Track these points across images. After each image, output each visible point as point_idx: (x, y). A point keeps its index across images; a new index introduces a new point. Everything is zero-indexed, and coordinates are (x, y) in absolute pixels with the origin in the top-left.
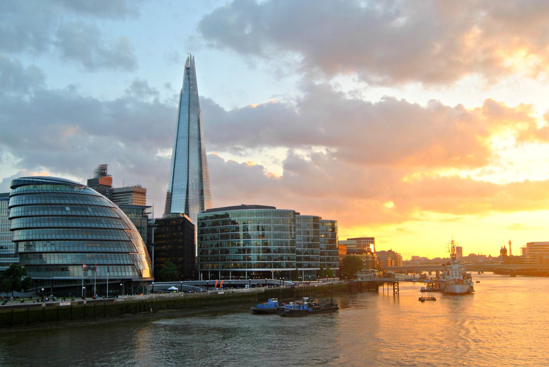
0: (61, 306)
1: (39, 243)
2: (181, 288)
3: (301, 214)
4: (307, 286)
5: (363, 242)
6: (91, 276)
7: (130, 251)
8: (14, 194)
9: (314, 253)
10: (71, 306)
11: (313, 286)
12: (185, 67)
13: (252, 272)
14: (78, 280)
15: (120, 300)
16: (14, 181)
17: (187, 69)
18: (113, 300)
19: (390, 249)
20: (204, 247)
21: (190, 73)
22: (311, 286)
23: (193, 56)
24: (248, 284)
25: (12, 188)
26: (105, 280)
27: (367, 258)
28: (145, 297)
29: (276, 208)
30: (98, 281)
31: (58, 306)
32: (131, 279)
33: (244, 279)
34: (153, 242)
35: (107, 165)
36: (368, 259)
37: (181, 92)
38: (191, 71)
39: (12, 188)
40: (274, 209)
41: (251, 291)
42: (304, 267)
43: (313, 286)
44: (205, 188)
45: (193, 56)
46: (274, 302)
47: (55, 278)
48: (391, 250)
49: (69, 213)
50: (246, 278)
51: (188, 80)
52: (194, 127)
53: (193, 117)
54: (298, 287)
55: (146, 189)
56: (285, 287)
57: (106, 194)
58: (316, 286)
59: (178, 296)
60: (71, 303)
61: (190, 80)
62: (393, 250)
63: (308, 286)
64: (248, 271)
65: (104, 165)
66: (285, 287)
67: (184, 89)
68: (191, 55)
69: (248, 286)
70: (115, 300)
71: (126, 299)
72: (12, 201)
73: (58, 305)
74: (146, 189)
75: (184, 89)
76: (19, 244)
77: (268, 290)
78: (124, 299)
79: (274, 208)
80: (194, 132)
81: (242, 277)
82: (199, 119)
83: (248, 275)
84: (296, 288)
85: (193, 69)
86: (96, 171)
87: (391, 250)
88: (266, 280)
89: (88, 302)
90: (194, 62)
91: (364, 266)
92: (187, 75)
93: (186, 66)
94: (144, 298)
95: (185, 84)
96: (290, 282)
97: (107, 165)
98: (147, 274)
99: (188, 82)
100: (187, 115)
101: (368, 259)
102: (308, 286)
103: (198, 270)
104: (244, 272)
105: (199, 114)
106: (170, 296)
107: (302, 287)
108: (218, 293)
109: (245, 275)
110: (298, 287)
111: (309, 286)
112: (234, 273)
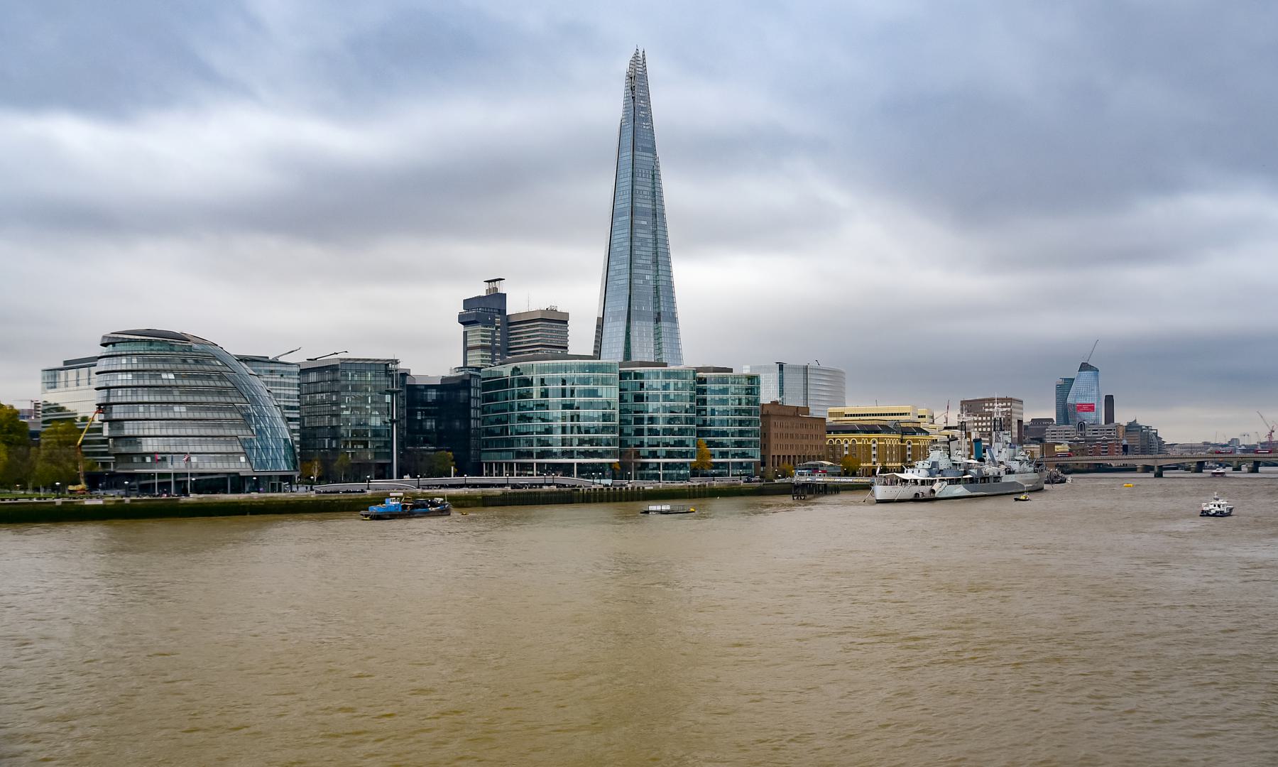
6: (183, 469)
7: (240, 434)
10: (115, 505)
11: (638, 488)
13: (544, 464)
18: (178, 499)
25: (103, 345)
26: (186, 475)
30: (176, 475)
31: (82, 506)
32: (237, 474)
33: (532, 475)
36: (880, 443)
43: (638, 488)
46: (394, 503)
50: (535, 474)
60: (104, 501)
62: (1140, 422)
71: (202, 498)
72: (102, 365)
73: (82, 504)
77: (510, 494)
80: (644, 204)
81: (529, 473)
83: (537, 470)
89: (132, 501)
94: (236, 498)
96: (609, 482)
101: (880, 443)
103: (482, 461)
109: (532, 470)
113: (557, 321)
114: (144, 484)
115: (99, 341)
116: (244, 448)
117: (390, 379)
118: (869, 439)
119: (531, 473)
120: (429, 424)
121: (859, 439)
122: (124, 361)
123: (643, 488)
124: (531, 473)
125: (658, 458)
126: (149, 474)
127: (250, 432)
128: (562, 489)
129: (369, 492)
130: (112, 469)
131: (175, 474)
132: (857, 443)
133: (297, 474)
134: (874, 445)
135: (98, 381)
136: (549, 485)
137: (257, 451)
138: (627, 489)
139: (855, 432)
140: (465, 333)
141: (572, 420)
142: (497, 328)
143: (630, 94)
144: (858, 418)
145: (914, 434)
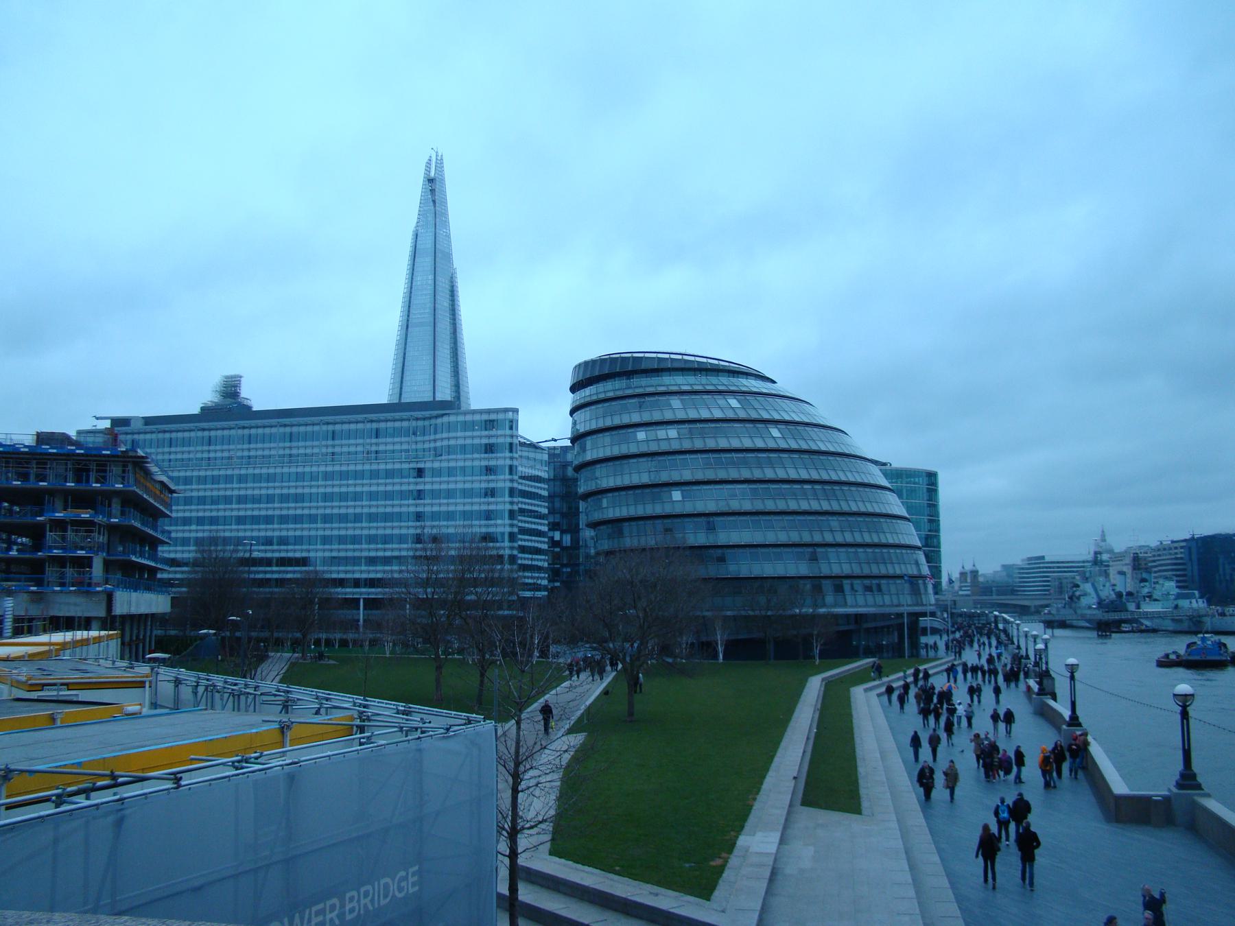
1: (645, 524)
17: (431, 181)
21: (437, 190)
23: (442, 156)
29: (892, 466)
38: (437, 187)
45: (442, 156)
51: (432, 204)
52: (444, 303)
61: (437, 205)
65: (232, 377)
82: (453, 286)
85: (443, 180)
86: (218, 389)
97: (241, 377)
99: (433, 208)
100: (431, 277)
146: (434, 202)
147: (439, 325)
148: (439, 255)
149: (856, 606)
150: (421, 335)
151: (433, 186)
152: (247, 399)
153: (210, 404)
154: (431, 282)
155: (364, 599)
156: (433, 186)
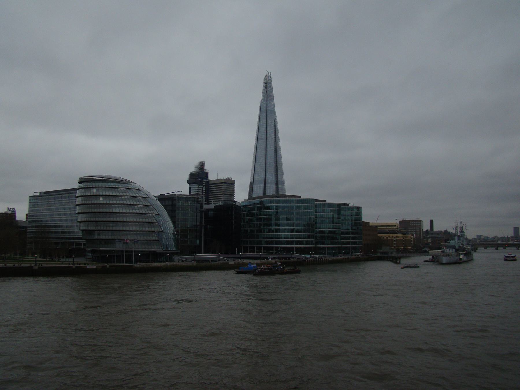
0: (88, 269)
2: (194, 258)
3: (327, 202)
4: (319, 260)
5: (412, 224)
7: (156, 230)
8: (81, 187)
9: (336, 232)
12: (264, 82)
13: (279, 247)
14: (114, 250)
15: (138, 266)
16: (81, 178)
17: (266, 83)
19: (445, 230)
20: (245, 228)
22: (324, 260)
23: (271, 73)
24: (270, 257)
25: (79, 183)
26: (132, 251)
27: (397, 237)
28: (161, 264)
30: (127, 251)
34: (203, 223)
35: (204, 162)
37: (261, 102)
38: (268, 85)
39: (80, 183)
40: (300, 198)
41: (261, 262)
42: (328, 244)
44: (279, 180)
45: (271, 73)
47: (101, 249)
48: (447, 230)
49: (102, 202)
50: (274, 252)
51: (266, 92)
52: (271, 130)
53: (271, 122)
54: (308, 260)
55: (234, 181)
56: (296, 259)
57: (204, 185)
58: (329, 259)
59: (191, 264)
60: (96, 266)
61: (268, 92)
63: (320, 260)
64: (275, 247)
66: (295, 260)
67: (263, 100)
68: (268, 72)
69: (270, 259)
70: (134, 266)
71: (144, 265)
72: (78, 193)
74: (234, 181)
75: (263, 100)
76: (81, 225)
78: (142, 265)
79: (300, 197)
82: (275, 123)
83: (275, 251)
84: (307, 260)
85: (271, 83)
87: (447, 230)
88: (277, 254)
89: (110, 266)
90: (271, 77)
91: (395, 244)
92: (265, 88)
93: (265, 82)
95: (263, 96)
97: (204, 162)
98: (172, 247)
99: (266, 94)
100: (265, 121)
102: (320, 260)
104: (273, 247)
105: (275, 120)
106: (184, 264)
107: (314, 260)
108: (228, 263)
109: (273, 250)
110: (309, 260)
111: (322, 260)
112: (265, 248)
113: (230, 184)
114: (100, 256)
115: (78, 181)
116: (158, 238)
117: (199, 205)
118: (393, 237)
119: (272, 251)
120: (208, 227)
121: (389, 237)
122: (95, 190)
123: (328, 259)
124: (272, 251)
125: (325, 245)
126: (112, 251)
127: (161, 230)
128: (299, 260)
129: (220, 262)
130: (83, 247)
131: (135, 251)
132: (389, 238)
133: (179, 251)
134: (395, 239)
135: (78, 201)
136: (293, 258)
137: (164, 239)
138: (323, 260)
139: (388, 233)
140: (190, 188)
141: (254, 227)
142: (204, 186)
143: (265, 90)
144: (385, 227)
145: (397, 233)
146: (267, 91)
147: (268, 139)
148: (269, 112)
149: (154, 249)
150: (262, 143)
151: (267, 86)
152: (207, 170)
153: (193, 172)
154: (265, 123)
155: (76, 243)
156: (267, 86)
